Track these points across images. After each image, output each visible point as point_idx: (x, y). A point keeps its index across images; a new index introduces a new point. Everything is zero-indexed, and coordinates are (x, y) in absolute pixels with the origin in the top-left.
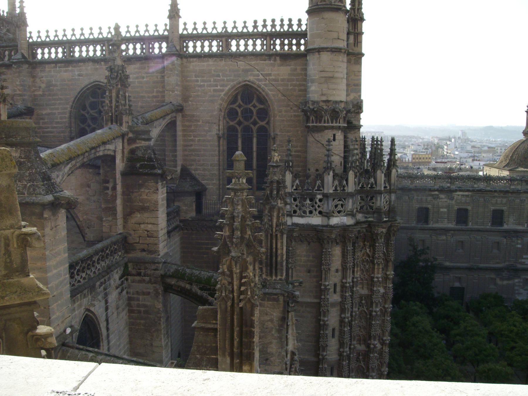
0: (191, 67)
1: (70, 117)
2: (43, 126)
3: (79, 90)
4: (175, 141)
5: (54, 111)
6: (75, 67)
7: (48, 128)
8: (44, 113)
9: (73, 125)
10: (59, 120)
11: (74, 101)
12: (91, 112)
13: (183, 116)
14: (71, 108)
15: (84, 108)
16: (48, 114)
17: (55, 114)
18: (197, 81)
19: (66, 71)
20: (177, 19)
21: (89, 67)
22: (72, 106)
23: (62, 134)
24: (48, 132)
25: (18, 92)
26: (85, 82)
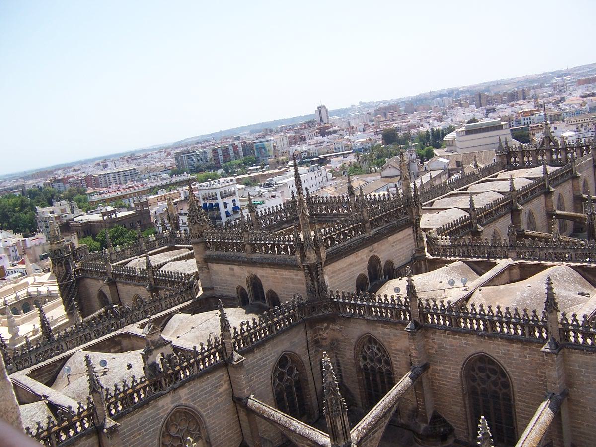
0: (574, 357)
1: (461, 377)
2: (438, 378)
3: (467, 356)
4: (561, 428)
5: (447, 369)
6: (461, 336)
7: (443, 381)
8: (438, 369)
9: (464, 383)
10: (451, 377)
11: (463, 365)
12: (481, 374)
13: (568, 399)
14: (462, 369)
15: (474, 370)
16: (442, 370)
17: (448, 371)
18: (581, 371)
19: (454, 338)
20: (555, 312)
21: (475, 339)
22: (462, 368)
23: (455, 389)
24: (444, 385)
25: (414, 354)
26: (471, 351)
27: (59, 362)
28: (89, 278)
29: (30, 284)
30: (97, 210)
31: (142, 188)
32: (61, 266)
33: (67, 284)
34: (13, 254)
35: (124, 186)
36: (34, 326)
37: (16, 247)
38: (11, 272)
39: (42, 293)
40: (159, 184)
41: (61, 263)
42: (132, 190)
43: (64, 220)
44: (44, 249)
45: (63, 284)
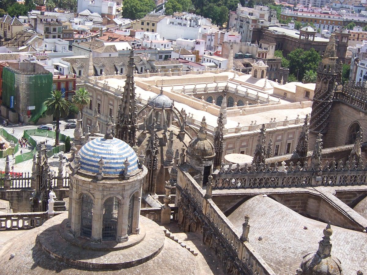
27: (359, 194)
28: (347, 105)
29: (229, 79)
30: (287, 26)
31: (338, 17)
32: (326, 83)
33: (323, 103)
34: (208, 43)
35: (320, 10)
36: (239, 124)
37: (213, 38)
38: (206, 60)
39: (239, 92)
40: (356, 19)
41: (327, 80)
42: (327, 16)
43: (260, 25)
44: (241, 48)
45: (320, 102)
